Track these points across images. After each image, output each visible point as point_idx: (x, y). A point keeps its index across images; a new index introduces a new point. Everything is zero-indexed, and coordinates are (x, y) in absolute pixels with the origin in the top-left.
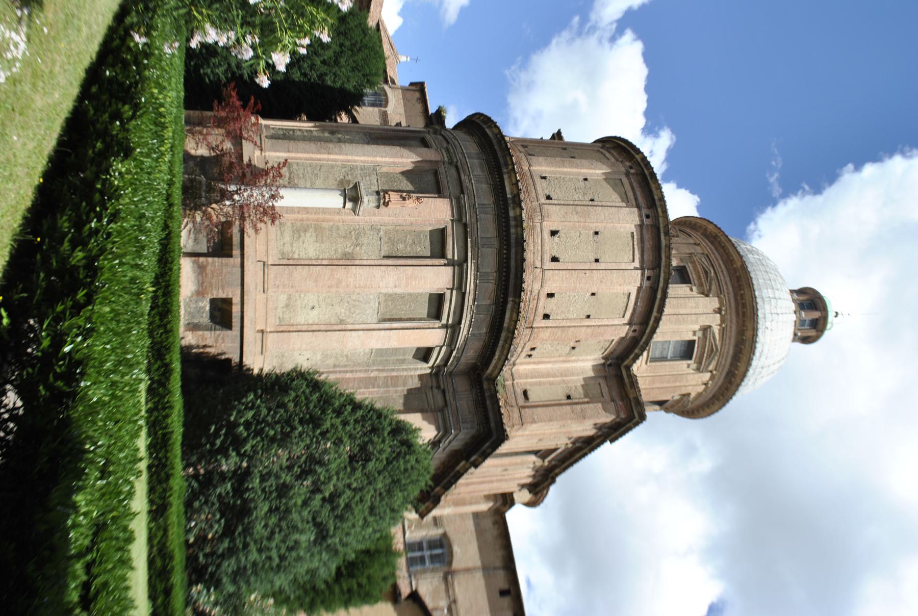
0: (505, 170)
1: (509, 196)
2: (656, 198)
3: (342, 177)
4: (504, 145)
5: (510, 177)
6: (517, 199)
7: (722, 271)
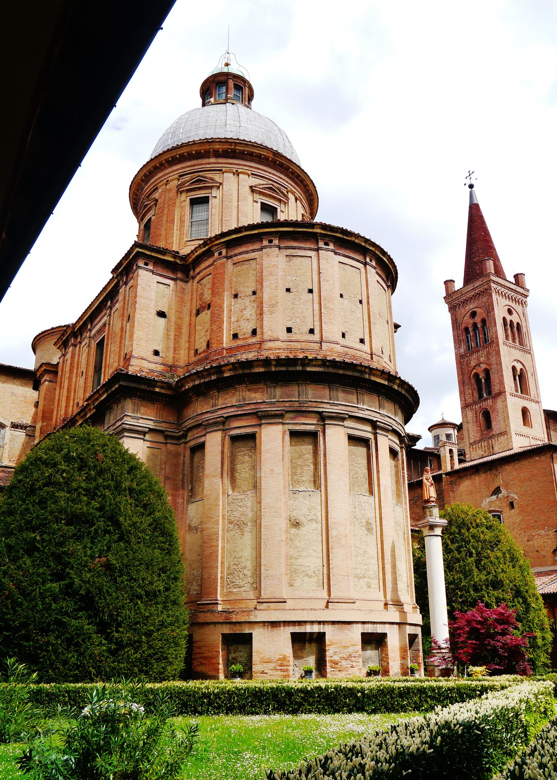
0: (367, 376)
1: (386, 383)
2: (363, 244)
3: (364, 529)
4: (343, 365)
5: (374, 375)
7: (270, 173)
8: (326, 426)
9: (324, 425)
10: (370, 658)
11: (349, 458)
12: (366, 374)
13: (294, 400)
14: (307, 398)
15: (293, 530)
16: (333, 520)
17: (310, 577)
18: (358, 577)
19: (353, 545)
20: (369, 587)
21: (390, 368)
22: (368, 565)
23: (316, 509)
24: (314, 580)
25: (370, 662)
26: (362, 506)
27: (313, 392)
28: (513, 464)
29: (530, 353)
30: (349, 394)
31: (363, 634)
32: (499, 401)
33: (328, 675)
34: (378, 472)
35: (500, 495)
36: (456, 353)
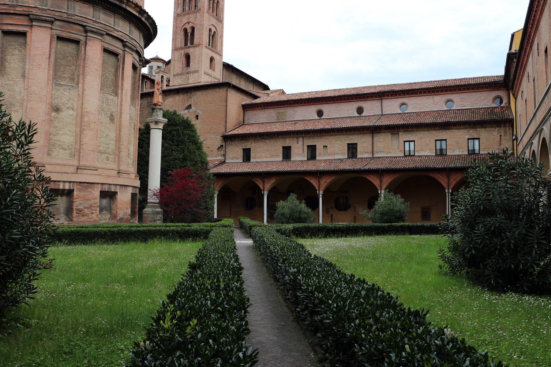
0: (124, 6)
1: (137, 14)
3: (108, 119)
5: (130, 6)
6: (142, 12)
8: (88, 37)
9: (86, 36)
10: (105, 208)
11: (103, 65)
12: (124, 4)
13: (63, 11)
14: (75, 12)
15: (54, 114)
16: (86, 110)
17: (65, 149)
18: (101, 152)
19: (99, 130)
20: (108, 160)
21: (140, 4)
22: (108, 145)
23: (73, 100)
24: (68, 152)
25: (104, 210)
26: (108, 102)
27: (80, 9)
28: (202, 91)
29: (221, 22)
30: (108, 16)
31: (101, 192)
32: (197, 49)
33: (74, 219)
34: (123, 79)
35: (190, 110)
36: (174, 11)
